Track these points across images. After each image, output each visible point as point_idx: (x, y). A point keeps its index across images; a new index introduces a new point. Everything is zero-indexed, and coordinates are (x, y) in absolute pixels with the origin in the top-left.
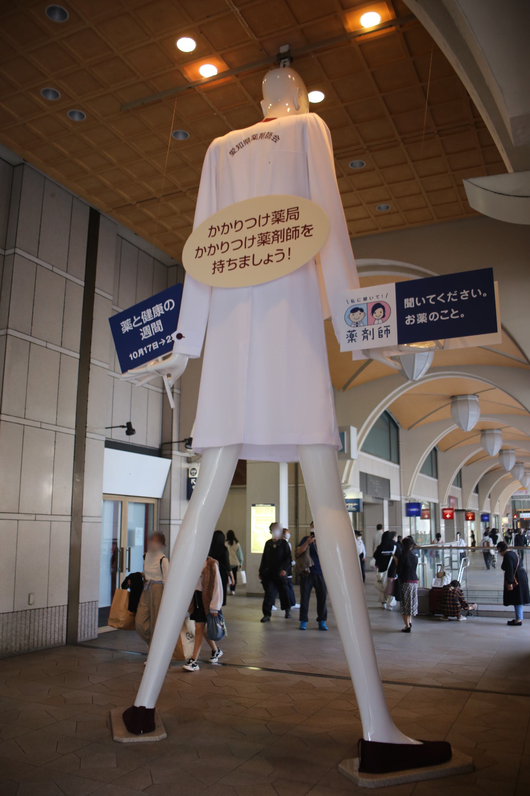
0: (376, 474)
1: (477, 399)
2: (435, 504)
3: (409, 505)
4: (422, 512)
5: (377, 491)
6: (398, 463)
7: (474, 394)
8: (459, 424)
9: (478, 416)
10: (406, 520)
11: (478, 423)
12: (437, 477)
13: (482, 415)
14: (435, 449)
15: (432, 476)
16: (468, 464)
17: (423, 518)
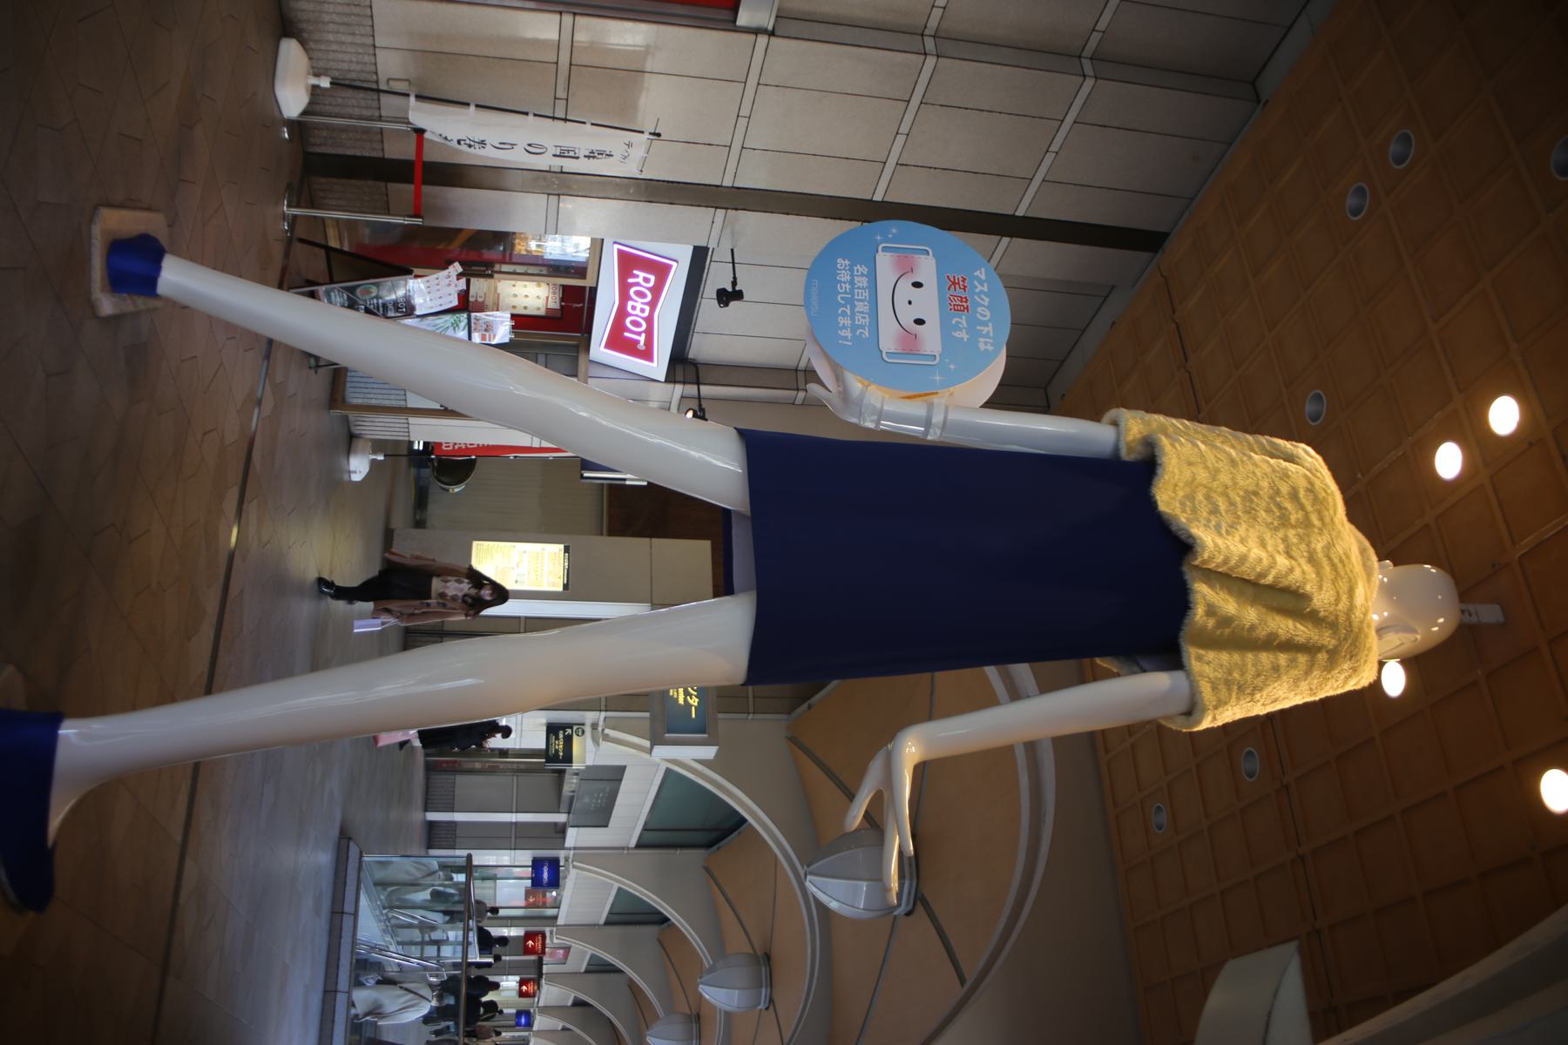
0: (621, 799)
1: (762, 1006)
2: (555, 918)
3: (554, 864)
4: (541, 890)
5: (586, 800)
6: (639, 846)
7: (771, 1001)
8: (712, 970)
9: (727, 1008)
10: (525, 857)
11: (713, 1007)
12: (607, 923)
13: (728, 1014)
14: (666, 920)
15: (610, 913)
16: (632, 985)
17: (528, 893)
